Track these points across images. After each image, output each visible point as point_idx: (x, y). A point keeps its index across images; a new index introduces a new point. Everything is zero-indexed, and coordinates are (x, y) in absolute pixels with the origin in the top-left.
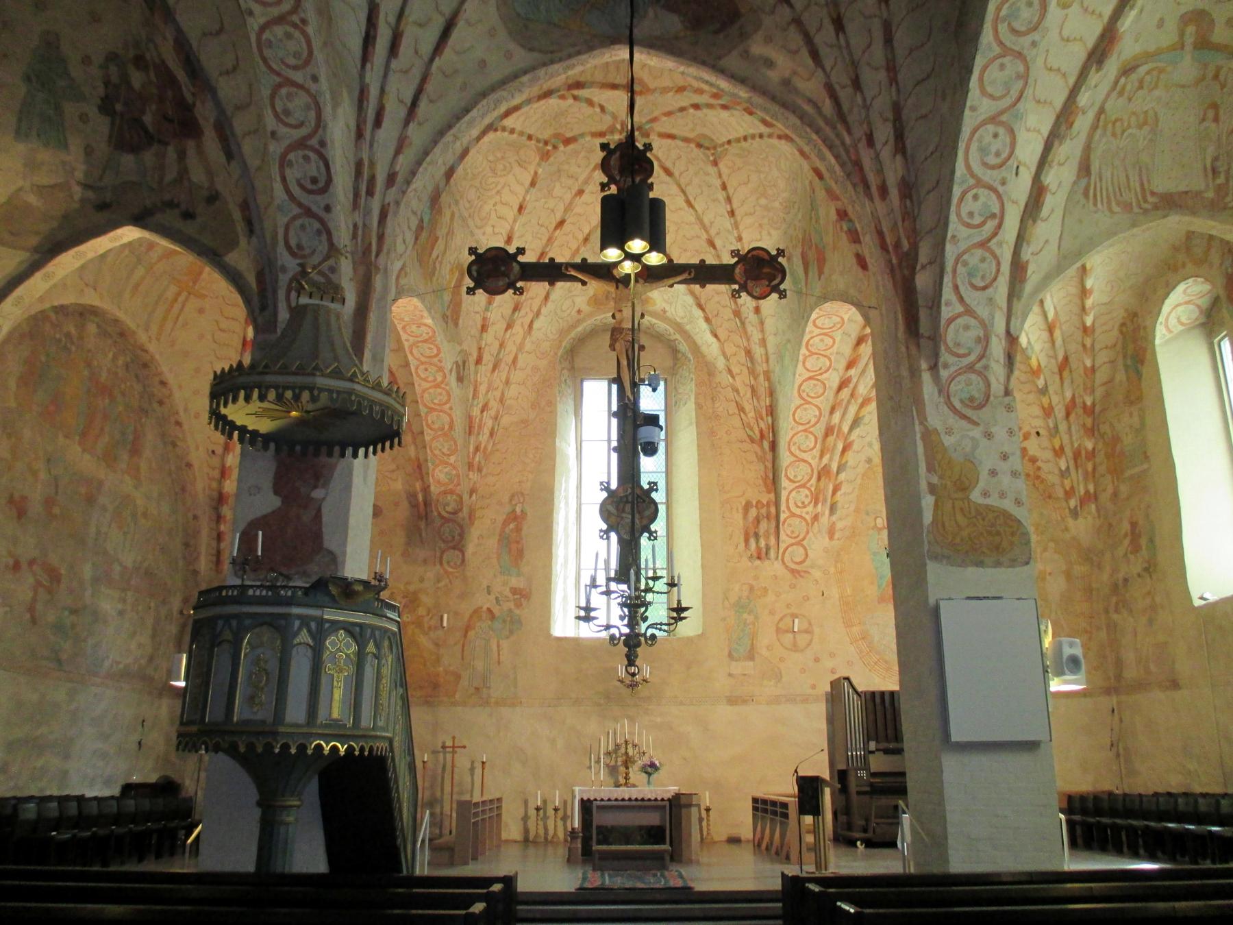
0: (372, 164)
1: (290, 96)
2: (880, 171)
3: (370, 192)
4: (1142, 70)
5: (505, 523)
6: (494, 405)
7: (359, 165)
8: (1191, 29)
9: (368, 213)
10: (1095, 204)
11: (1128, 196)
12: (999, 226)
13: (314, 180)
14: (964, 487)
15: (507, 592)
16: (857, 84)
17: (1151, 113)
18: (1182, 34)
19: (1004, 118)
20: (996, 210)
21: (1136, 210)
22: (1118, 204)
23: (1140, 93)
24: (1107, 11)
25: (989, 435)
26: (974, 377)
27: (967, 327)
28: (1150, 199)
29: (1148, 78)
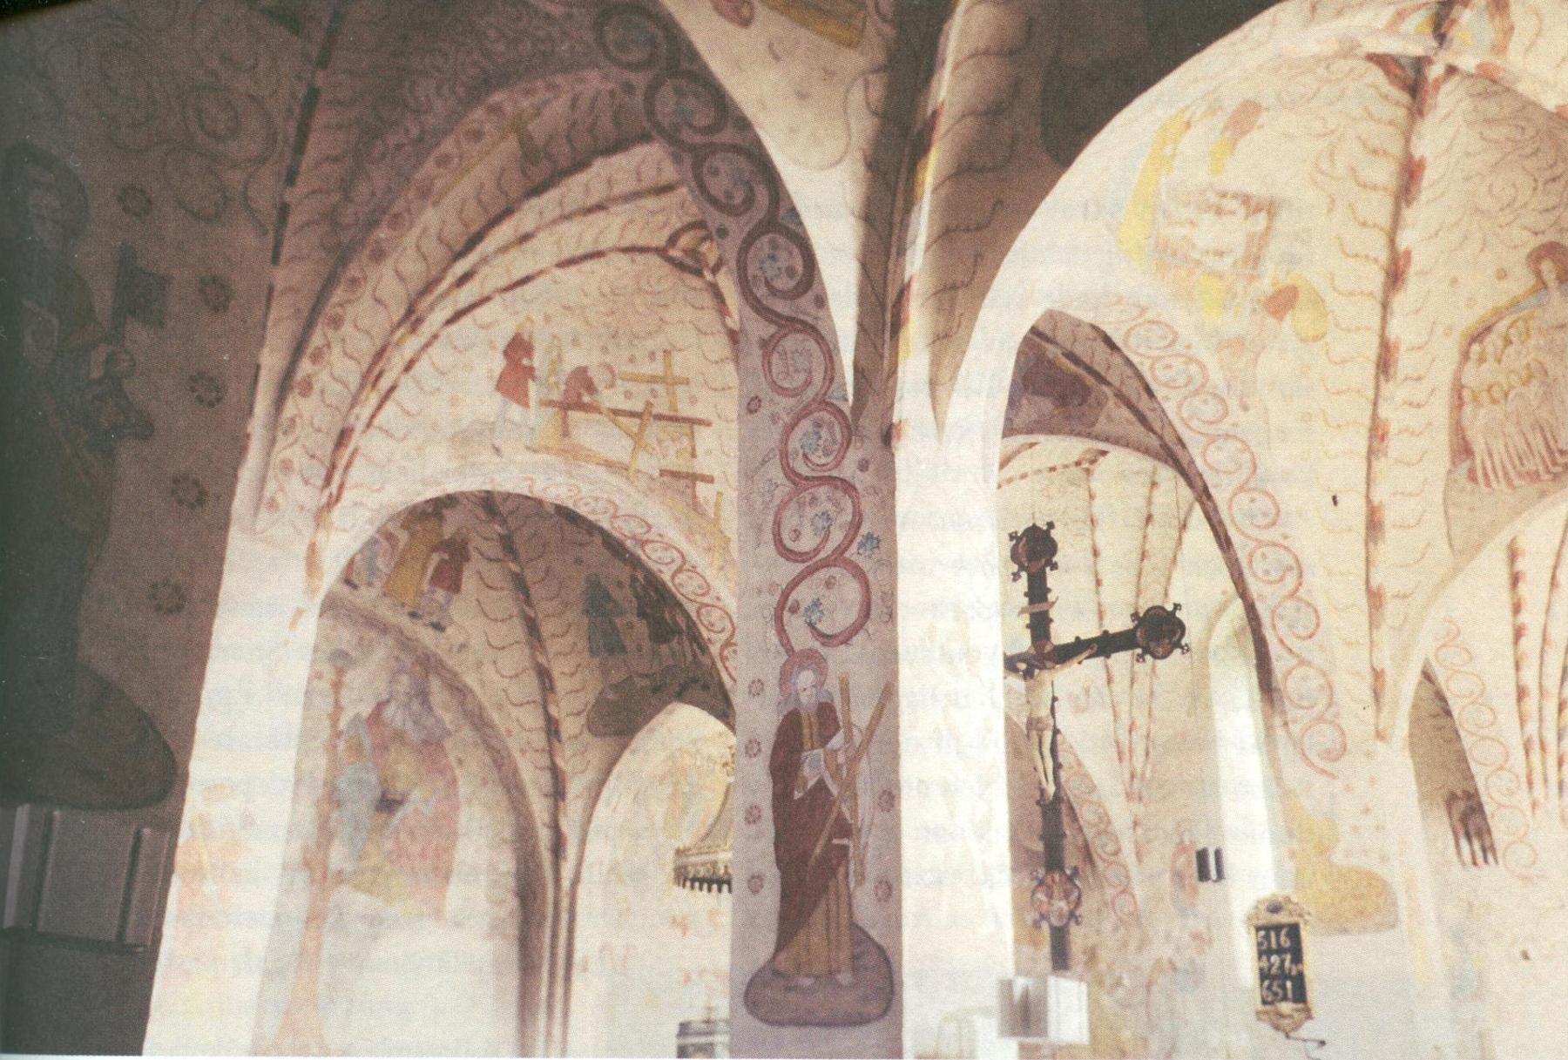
1: (708, 613)
4: (1502, 326)
5: (1175, 856)
6: (1141, 721)
8: (1547, 267)
10: (1488, 485)
11: (1530, 466)
12: (1301, 575)
14: (1324, 850)
15: (1186, 938)
17: (1533, 365)
18: (1538, 274)
19: (1252, 485)
20: (1290, 561)
21: (1547, 477)
22: (1520, 475)
23: (1511, 350)
24: (1375, 321)
25: (1348, 788)
26: (1324, 727)
27: (1305, 679)
28: (1560, 460)
29: (1513, 331)
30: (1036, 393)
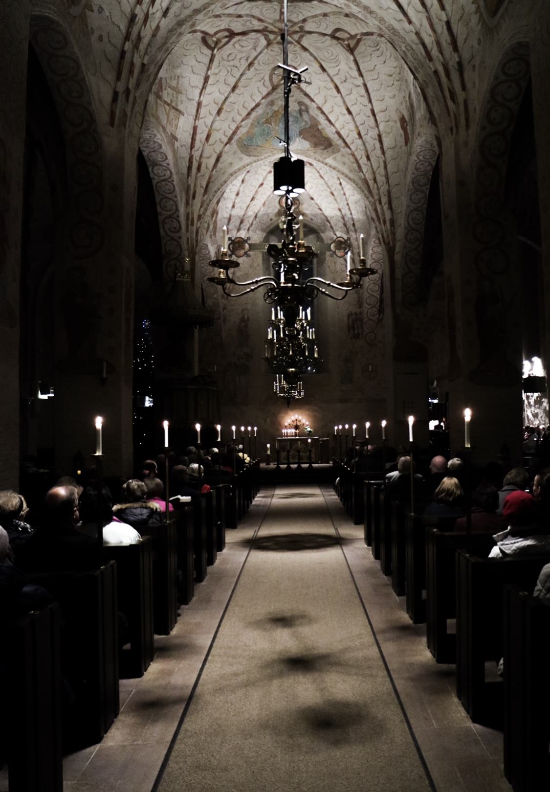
0: (193, 213)
2: (383, 214)
3: (192, 225)
7: (188, 215)
9: (192, 232)
13: (175, 228)
16: (375, 180)
30: (304, 138)
